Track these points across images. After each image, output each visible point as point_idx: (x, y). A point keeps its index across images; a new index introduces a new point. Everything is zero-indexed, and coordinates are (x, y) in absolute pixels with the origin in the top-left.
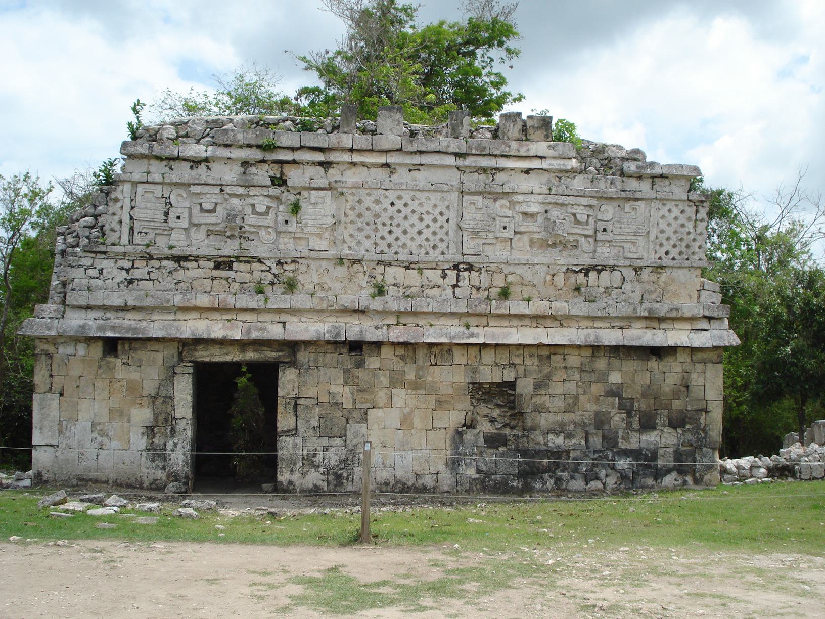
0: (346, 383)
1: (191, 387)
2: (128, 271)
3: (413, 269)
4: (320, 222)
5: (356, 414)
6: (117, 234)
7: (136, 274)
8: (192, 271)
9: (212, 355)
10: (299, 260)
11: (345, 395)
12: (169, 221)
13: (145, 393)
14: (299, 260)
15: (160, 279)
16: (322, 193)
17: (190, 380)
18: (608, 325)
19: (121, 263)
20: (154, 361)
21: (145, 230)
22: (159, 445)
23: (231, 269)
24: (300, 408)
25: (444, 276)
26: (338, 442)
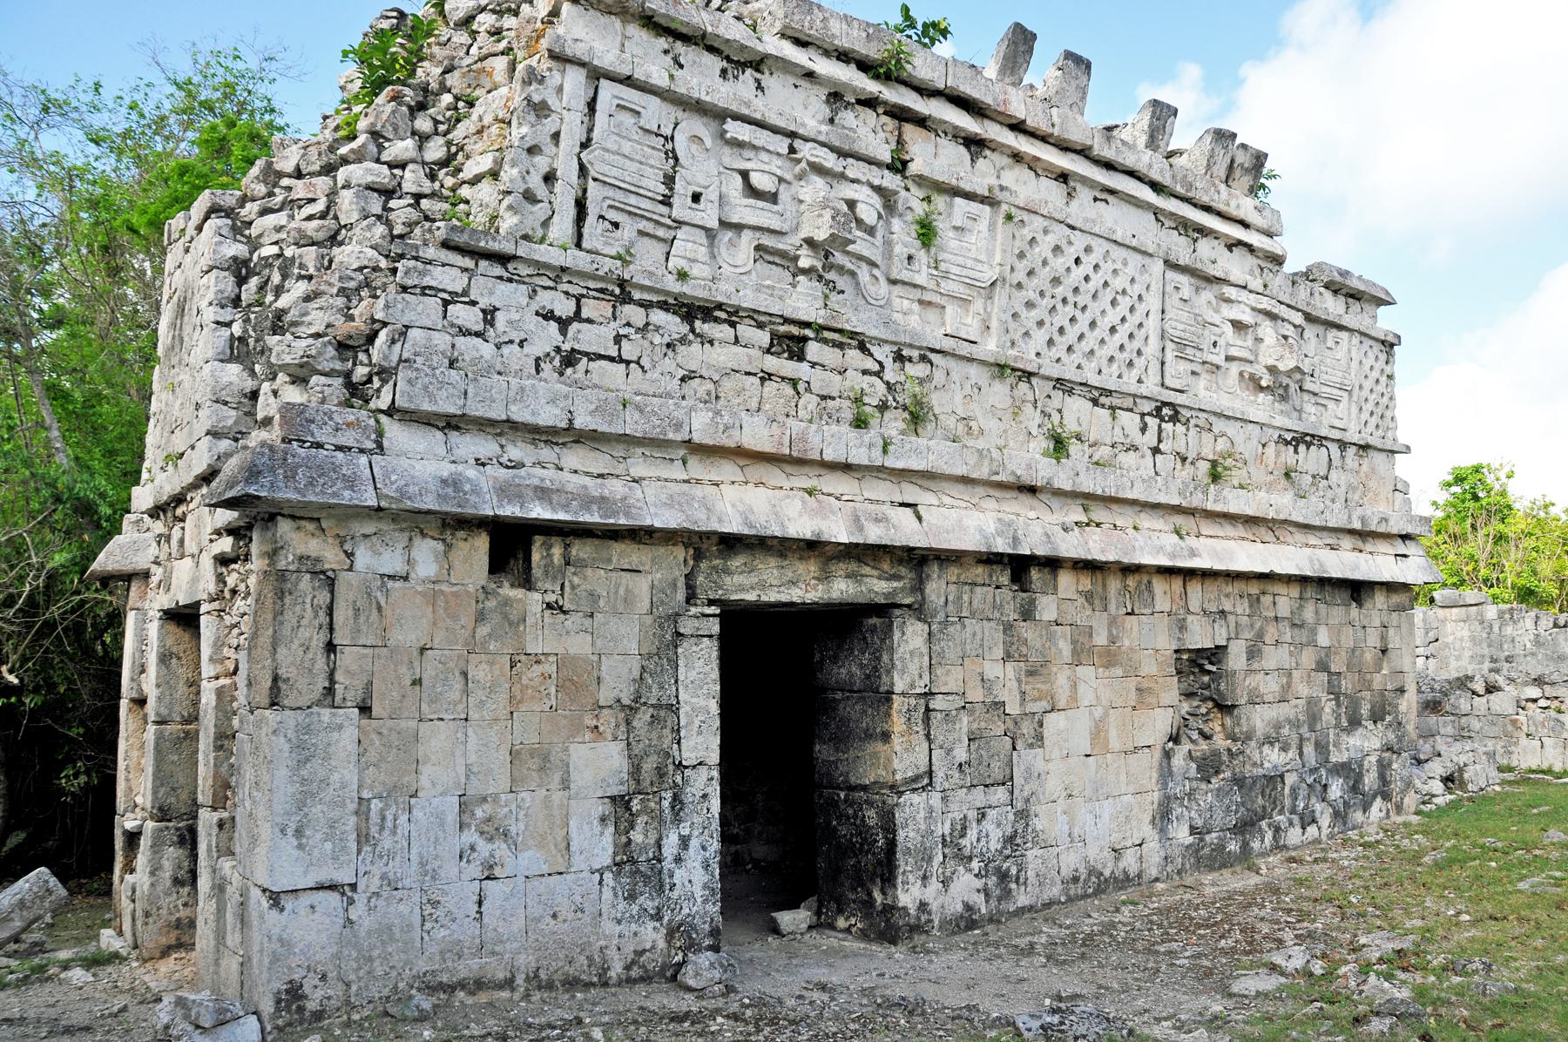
0: (1007, 657)
1: (715, 674)
2: (564, 324)
3: (1103, 406)
4: (972, 274)
5: (1027, 728)
6: (540, 211)
7: (587, 337)
8: (724, 352)
9: (763, 586)
10: (932, 356)
11: (1006, 678)
12: (676, 201)
13: (605, 696)
14: (932, 356)
15: (645, 362)
16: (974, 207)
17: (715, 654)
18: (1319, 542)
19: (546, 299)
20: (629, 599)
21: (613, 215)
22: (644, 848)
23: (800, 357)
24: (936, 718)
25: (1144, 429)
26: (1000, 794)
